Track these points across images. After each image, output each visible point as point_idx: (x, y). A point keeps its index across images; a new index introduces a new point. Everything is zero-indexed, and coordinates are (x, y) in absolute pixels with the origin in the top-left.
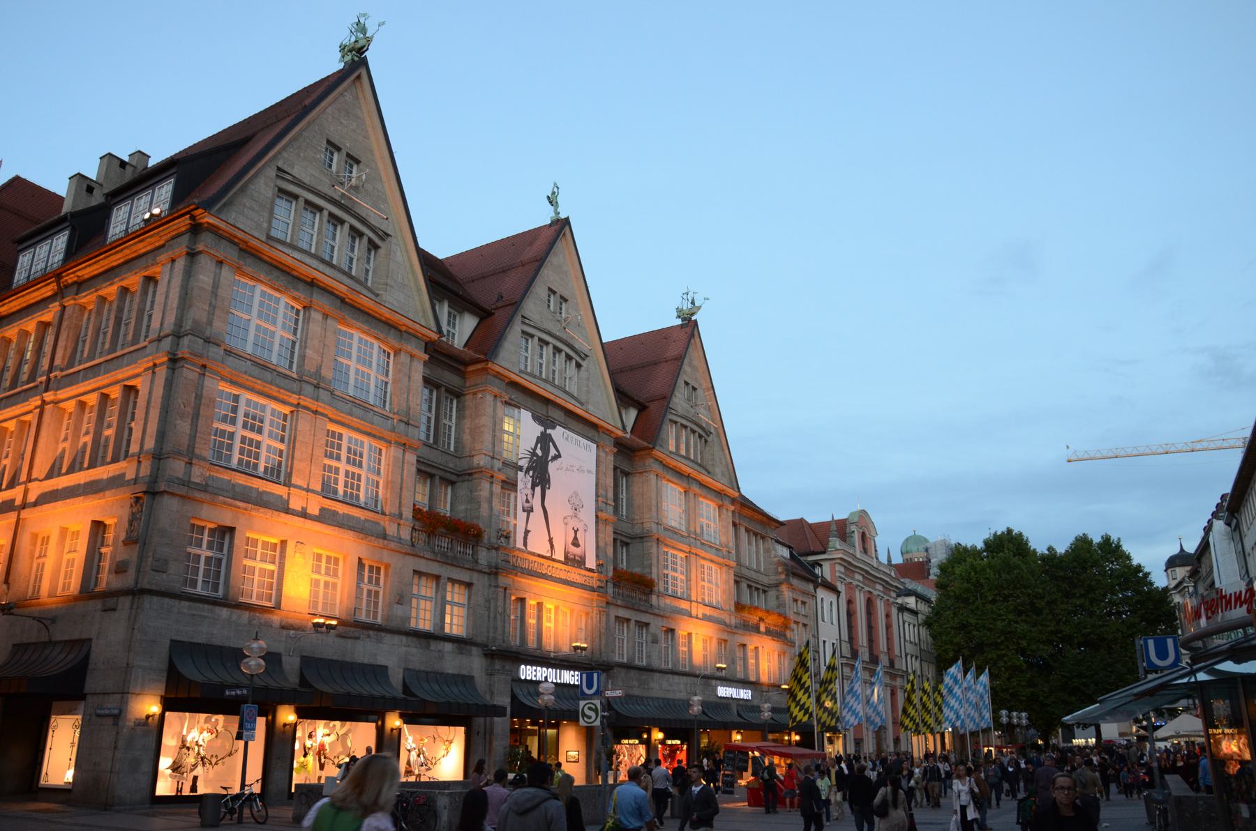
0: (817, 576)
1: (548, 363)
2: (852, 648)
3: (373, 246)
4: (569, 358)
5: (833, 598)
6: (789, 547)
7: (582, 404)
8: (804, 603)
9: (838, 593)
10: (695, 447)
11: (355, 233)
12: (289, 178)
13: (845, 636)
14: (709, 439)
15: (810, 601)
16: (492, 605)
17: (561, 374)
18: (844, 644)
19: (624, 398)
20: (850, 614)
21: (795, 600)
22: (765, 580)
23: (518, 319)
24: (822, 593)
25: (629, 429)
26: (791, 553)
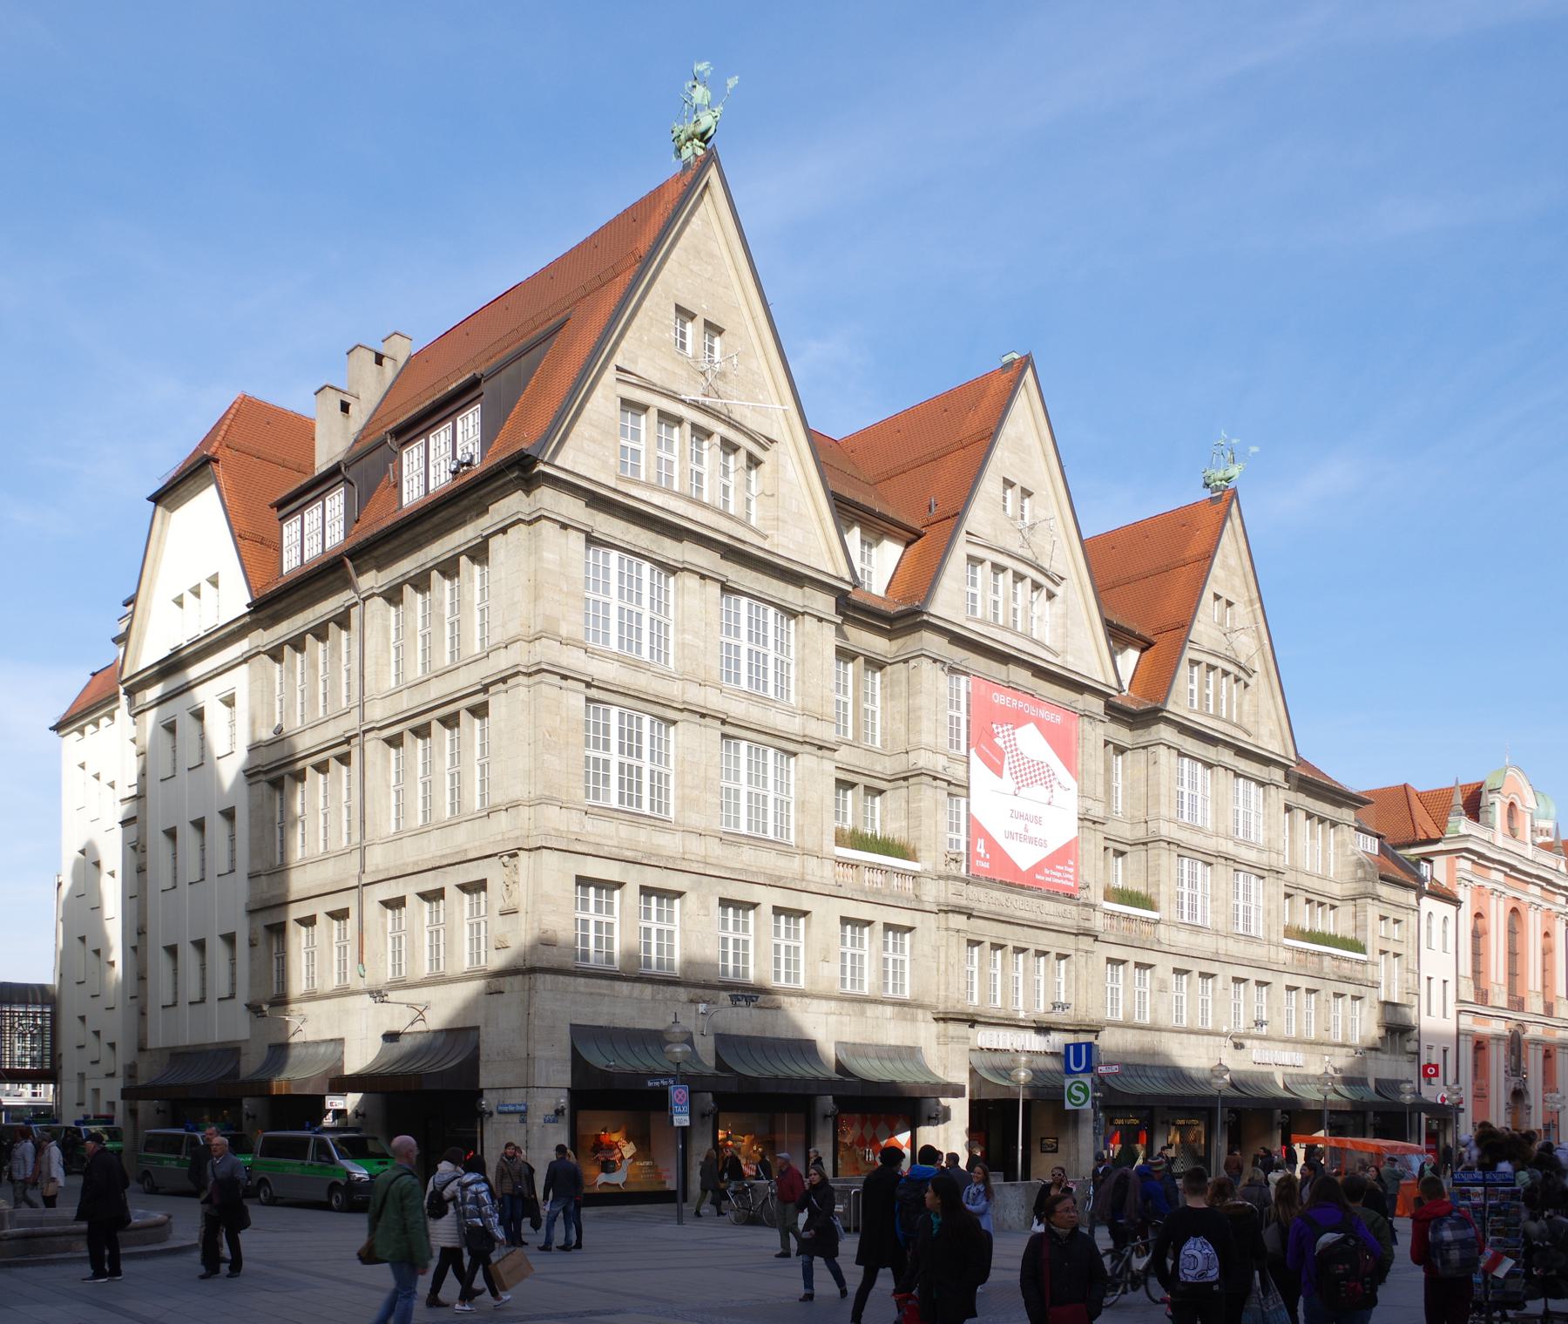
0: (1421, 880)
1: (1006, 600)
2: (1477, 988)
3: (754, 462)
4: (1036, 586)
5: (1449, 909)
6: (1378, 837)
7: (1056, 654)
8: (1397, 921)
9: (1457, 903)
10: (1229, 699)
11: (729, 447)
12: (633, 379)
13: (1466, 968)
14: (1251, 682)
15: (1412, 918)
16: (942, 955)
17: (1026, 612)
18: (1463, 982)
19: (1118, 636)
20: (1477, 935)
21: (1383, 918)
22: (1336, 890)
23: (962, 536)
24: (1428, 904)
25: (1126, 685)
26: (1381, 846)
